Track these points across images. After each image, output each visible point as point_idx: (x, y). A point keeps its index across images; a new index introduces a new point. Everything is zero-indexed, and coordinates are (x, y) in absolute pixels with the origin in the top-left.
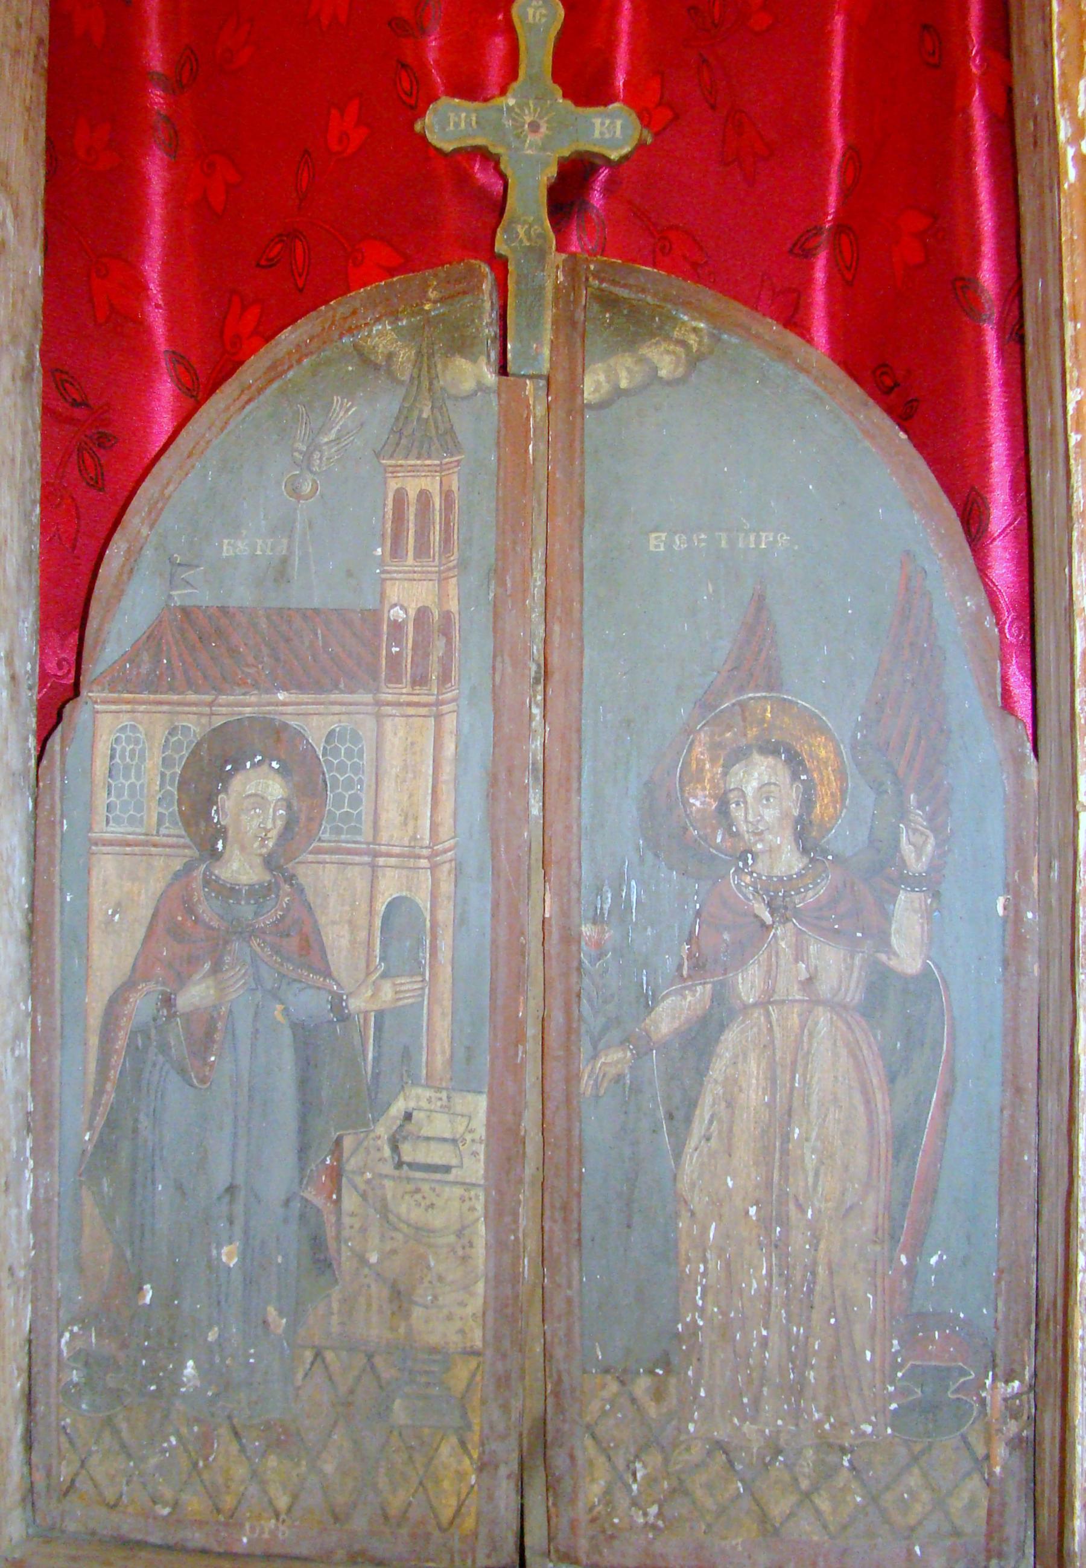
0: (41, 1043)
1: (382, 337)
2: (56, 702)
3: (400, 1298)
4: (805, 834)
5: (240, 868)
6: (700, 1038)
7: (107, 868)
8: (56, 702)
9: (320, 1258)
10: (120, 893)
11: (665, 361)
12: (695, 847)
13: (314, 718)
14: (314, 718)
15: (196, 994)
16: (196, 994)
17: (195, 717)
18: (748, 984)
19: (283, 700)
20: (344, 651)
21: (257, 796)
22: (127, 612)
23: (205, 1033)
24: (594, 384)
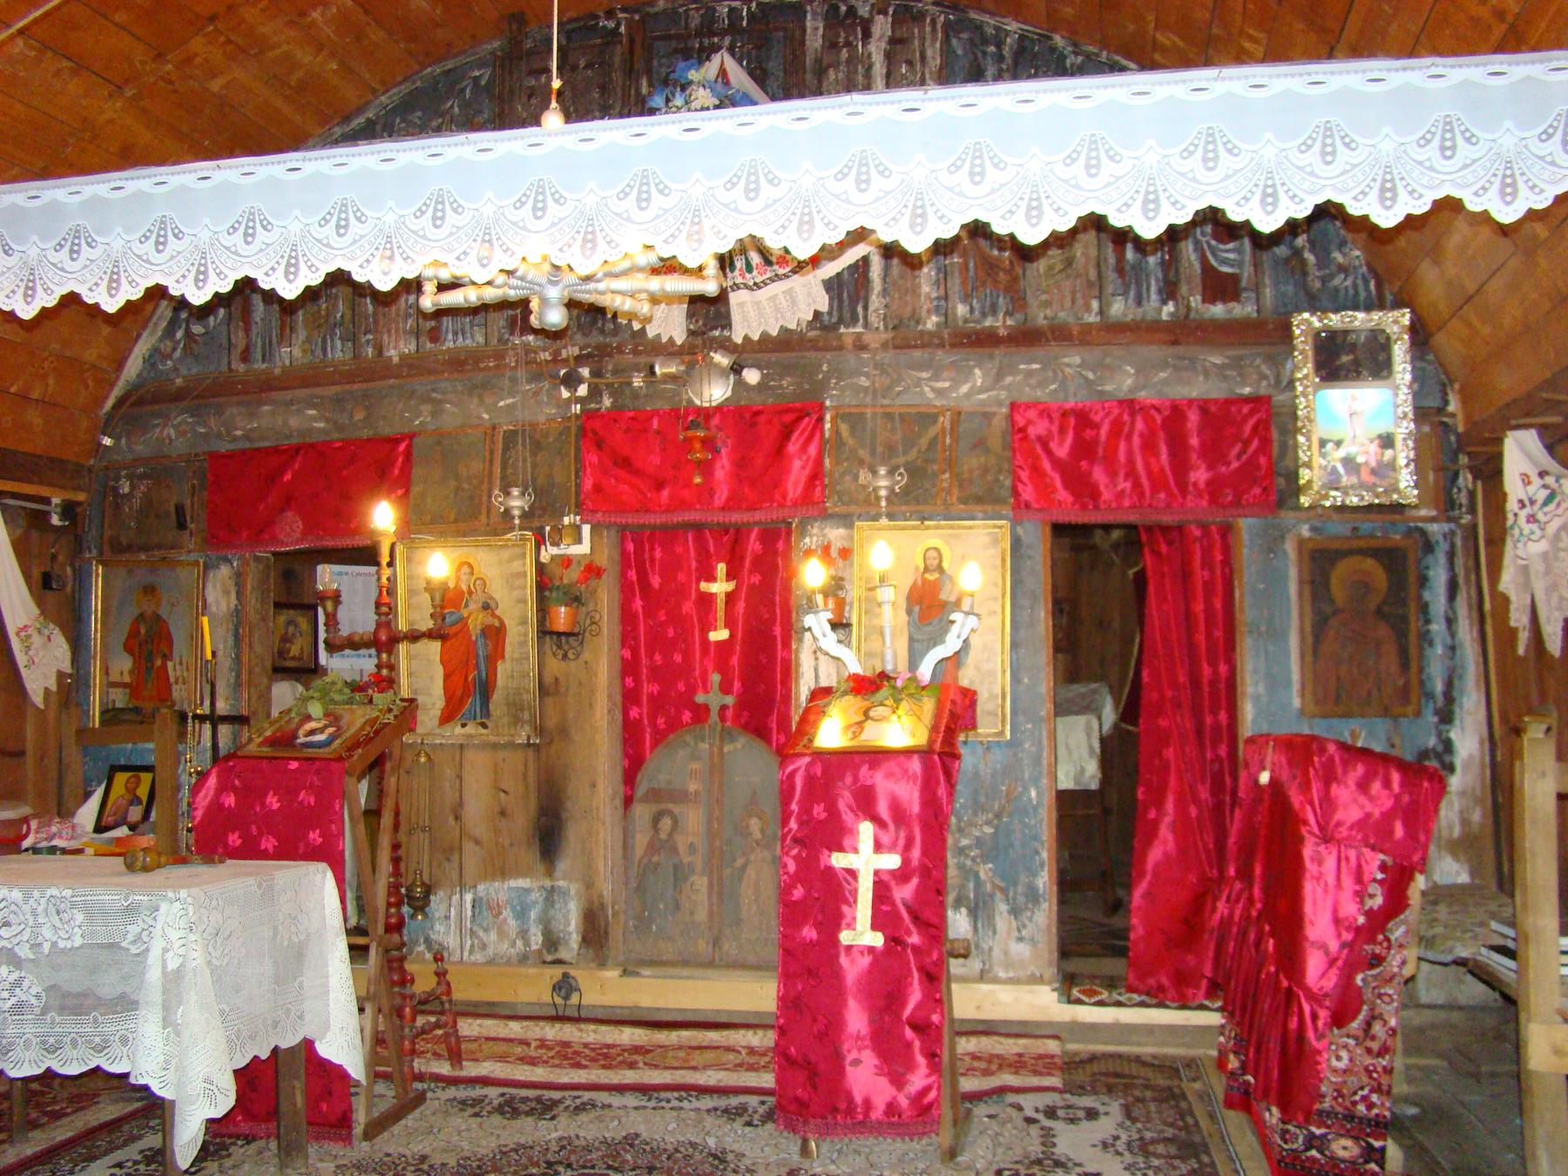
0: (626, 869)
1: (688, 738)
2: (628, 801)
3: (692, 913)
4: (762, 831)
5: (663, 836)
6: (743, 868)
7: (638, 836)
8: (628, 801)
9: (677, 906)
10: (641, 840)
11: (739, 745)
12: (744, 833)
13: (676, 809)
14: (676, 809)
15: (655, 859)
16: (655, 859)
17: (654, 808)
18: (752, 858)
19: (671, 806)
20: (682, 797)
21: (666, 823)
22: (642, 789)
23: (657, 865)
24: (726, 749)
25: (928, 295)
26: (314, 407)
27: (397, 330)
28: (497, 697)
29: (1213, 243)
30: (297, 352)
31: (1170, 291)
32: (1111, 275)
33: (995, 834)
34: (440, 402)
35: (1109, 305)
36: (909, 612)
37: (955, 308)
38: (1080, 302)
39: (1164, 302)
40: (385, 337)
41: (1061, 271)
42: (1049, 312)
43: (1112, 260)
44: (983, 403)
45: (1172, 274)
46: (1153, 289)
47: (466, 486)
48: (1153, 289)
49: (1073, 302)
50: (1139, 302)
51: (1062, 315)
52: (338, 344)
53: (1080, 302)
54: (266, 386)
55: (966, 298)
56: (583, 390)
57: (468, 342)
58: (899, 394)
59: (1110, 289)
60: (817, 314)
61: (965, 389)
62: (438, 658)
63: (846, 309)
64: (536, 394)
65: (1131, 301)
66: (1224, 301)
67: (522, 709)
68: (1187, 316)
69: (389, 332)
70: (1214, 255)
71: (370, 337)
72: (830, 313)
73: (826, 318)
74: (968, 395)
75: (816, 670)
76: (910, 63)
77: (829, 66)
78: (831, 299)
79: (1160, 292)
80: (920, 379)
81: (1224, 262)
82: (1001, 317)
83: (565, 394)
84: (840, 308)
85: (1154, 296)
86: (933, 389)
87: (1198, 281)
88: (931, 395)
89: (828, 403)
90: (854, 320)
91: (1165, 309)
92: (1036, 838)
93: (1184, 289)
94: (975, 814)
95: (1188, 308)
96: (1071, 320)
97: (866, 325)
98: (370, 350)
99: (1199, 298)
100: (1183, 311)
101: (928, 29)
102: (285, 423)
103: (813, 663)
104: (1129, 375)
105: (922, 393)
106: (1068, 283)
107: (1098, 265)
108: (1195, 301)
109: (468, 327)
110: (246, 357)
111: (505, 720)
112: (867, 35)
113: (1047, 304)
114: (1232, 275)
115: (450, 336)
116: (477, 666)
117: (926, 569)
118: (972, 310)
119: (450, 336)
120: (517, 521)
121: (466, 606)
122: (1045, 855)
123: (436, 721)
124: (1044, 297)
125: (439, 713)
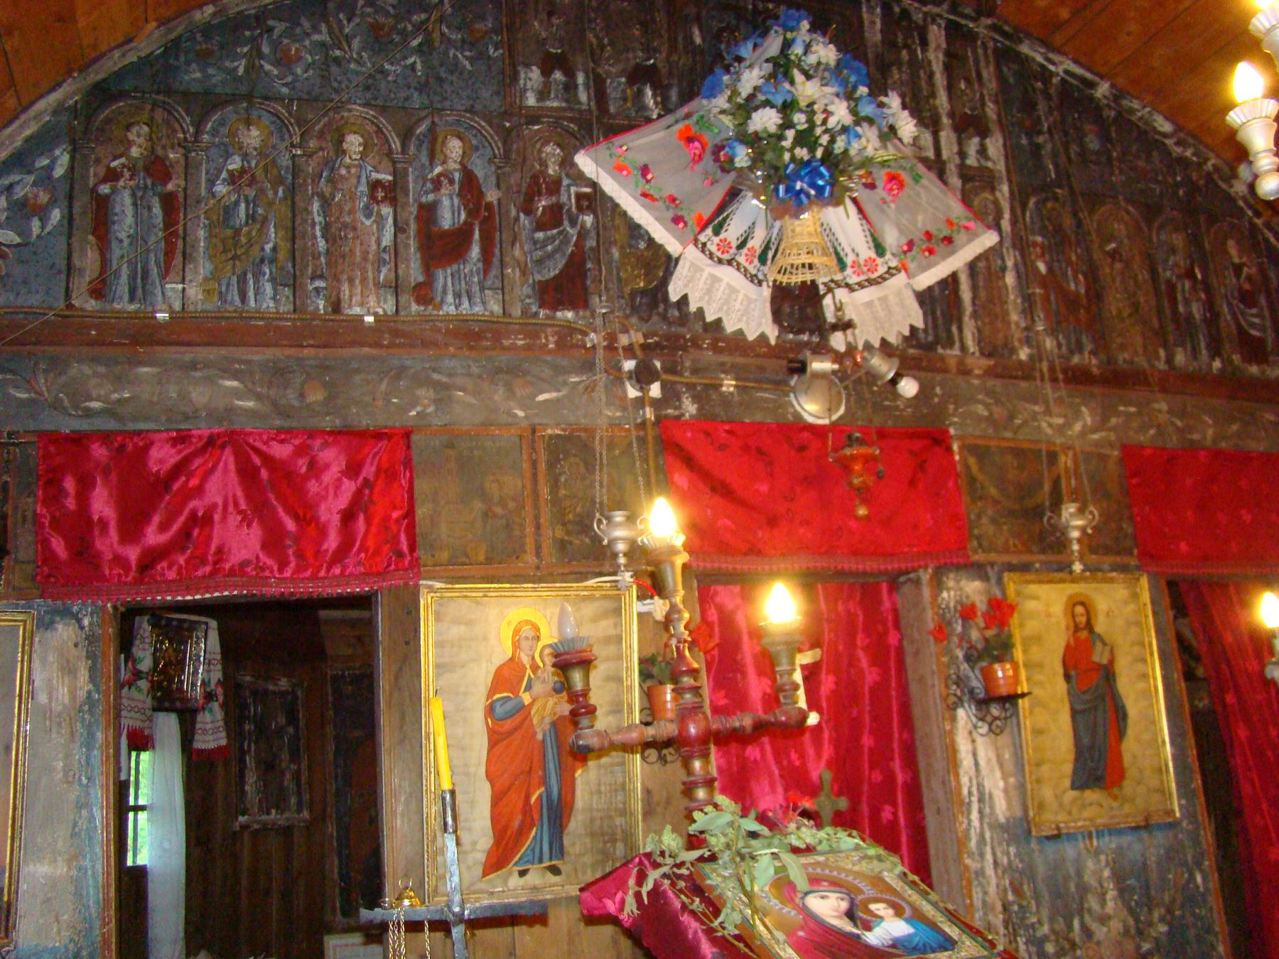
25: (1017, 324)
26: (235, 376)
27: (364, 280)
28: (576, 824)
30: (194, 292)
33: (1169, 933)
34: (446, 387)
36: (1067, 677)
40: (345, 288)
44: (1097, 444)
46: (1203, 344)
47: (499, 510)
50: (1195, 353)
52: (268, 288)
54: (143, 337)
56: (655, 390)
57: (478, 309)
58: (1020, 427)
59: (1171, 338)
60: (913, 329)
61: (1078, 427)
62: (482, 770)
63: (941, 328)
64: (590, 388)
67: (613, 841)
69: (351, 281)
71: (320, 284)
72: (925, 331)
73: (922, 335)
74: (1083, 433)
75: (975, 754)
77: (892, 64)
78: (925, 315)
79: (1208, 347)
80: (1035, 413)
83: (633, 393)
84: (935, 327)
85: (1204, 352)
86: (1050, 425)
88: (1049, 431)
89: (952, 431)
90: (950, 343)
92: (1209, 930)
94: (1150, 910)
97: (963, 348)
98: (321, 304)
101: (980, 51)
102: (183, 396)
103: (970, 747)
104: (1210, 426)
105: (1039, 427)
108: (1236, 358)
109: (476, 289)
110: (99, 290)
111: (587, 859)
112: (924, 43)
115: (450, 298)
116: (544, 781)
117: (1077, 628)
118: (1059, 345)
119: (450, 298)
120: (622, 560)
121: (529, 688)
122: (1221, 948)
123: (479, 870)
125: (481, 857)
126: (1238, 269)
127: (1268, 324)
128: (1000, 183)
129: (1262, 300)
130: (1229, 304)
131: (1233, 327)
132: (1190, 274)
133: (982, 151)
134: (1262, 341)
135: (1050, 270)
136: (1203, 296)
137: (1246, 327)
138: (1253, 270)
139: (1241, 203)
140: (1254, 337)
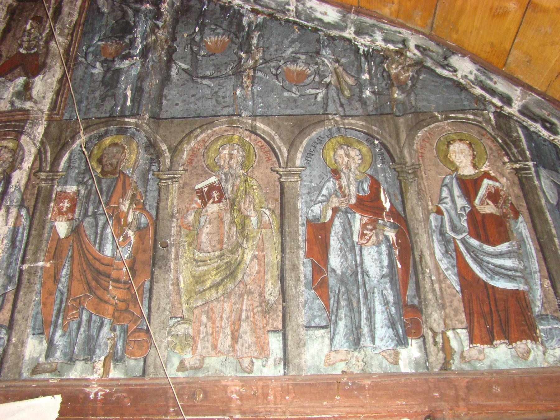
29: (474, 242)
31: (410, 322)
32: (303, 294)
35: (301, 344)
37: (23, 344)
38: (248, 338)
39: (402, 342)
41: (216, 286)
42: (189, 357)
43: (305, 269)
45: (411, 291)
46: (380, 318)
48: (380, 318)
49: (235, 339)
51: (213, 362)
53: (248, 338)
55: (44, 329)
59: (301, 317)
65: (340, 338)
66: (510, 340)
68: (445, 366)
70: (480, 263)
76: (39, 20)
81: (498, 272)
82: (99, 365)
85: (382, 331)
87: (458, 303)
91: (404, 352)
93: (435, 318)
95: (446, 349)
96: (230, 372)
99: (463, 334)
100: (437, 358)
106: (227, 306)
107: (282, 277)
108: (459, 338)
113: (189, 341)
114: (516, 293)
118: (49, 353)
124: (181, 329)
126: (469, 187)
127: (535, 265)
128: (34, 125)
129: (522, 227)
130: (446, 241)
131: (453, 279)
132: (369, 204)
133: (25, 93)
134: (520, 300)
135: (76, 231)
136: (392, 235)
137: (483, 276)
138: (504, 183)
139: (478, 91)
140: (505, 291)
